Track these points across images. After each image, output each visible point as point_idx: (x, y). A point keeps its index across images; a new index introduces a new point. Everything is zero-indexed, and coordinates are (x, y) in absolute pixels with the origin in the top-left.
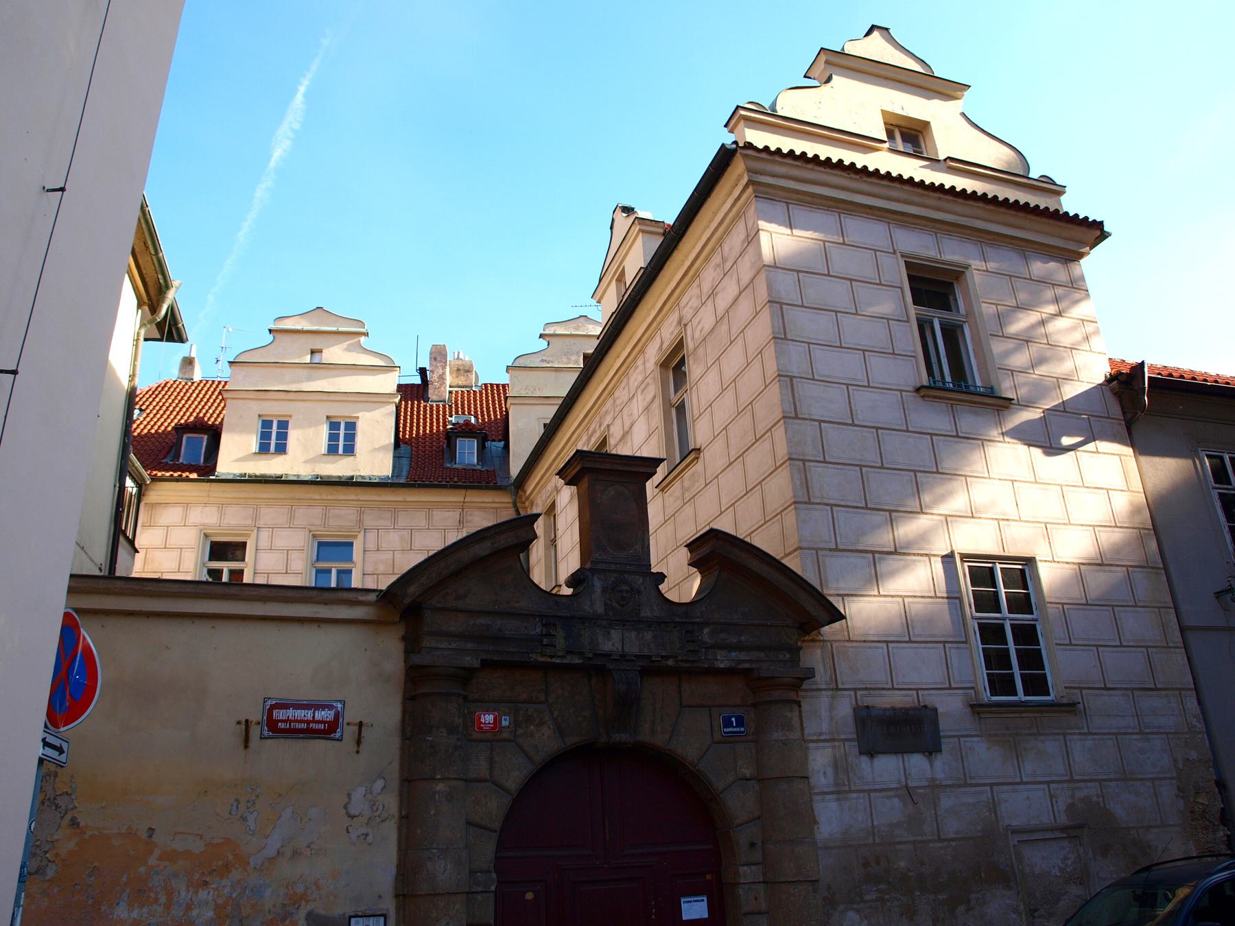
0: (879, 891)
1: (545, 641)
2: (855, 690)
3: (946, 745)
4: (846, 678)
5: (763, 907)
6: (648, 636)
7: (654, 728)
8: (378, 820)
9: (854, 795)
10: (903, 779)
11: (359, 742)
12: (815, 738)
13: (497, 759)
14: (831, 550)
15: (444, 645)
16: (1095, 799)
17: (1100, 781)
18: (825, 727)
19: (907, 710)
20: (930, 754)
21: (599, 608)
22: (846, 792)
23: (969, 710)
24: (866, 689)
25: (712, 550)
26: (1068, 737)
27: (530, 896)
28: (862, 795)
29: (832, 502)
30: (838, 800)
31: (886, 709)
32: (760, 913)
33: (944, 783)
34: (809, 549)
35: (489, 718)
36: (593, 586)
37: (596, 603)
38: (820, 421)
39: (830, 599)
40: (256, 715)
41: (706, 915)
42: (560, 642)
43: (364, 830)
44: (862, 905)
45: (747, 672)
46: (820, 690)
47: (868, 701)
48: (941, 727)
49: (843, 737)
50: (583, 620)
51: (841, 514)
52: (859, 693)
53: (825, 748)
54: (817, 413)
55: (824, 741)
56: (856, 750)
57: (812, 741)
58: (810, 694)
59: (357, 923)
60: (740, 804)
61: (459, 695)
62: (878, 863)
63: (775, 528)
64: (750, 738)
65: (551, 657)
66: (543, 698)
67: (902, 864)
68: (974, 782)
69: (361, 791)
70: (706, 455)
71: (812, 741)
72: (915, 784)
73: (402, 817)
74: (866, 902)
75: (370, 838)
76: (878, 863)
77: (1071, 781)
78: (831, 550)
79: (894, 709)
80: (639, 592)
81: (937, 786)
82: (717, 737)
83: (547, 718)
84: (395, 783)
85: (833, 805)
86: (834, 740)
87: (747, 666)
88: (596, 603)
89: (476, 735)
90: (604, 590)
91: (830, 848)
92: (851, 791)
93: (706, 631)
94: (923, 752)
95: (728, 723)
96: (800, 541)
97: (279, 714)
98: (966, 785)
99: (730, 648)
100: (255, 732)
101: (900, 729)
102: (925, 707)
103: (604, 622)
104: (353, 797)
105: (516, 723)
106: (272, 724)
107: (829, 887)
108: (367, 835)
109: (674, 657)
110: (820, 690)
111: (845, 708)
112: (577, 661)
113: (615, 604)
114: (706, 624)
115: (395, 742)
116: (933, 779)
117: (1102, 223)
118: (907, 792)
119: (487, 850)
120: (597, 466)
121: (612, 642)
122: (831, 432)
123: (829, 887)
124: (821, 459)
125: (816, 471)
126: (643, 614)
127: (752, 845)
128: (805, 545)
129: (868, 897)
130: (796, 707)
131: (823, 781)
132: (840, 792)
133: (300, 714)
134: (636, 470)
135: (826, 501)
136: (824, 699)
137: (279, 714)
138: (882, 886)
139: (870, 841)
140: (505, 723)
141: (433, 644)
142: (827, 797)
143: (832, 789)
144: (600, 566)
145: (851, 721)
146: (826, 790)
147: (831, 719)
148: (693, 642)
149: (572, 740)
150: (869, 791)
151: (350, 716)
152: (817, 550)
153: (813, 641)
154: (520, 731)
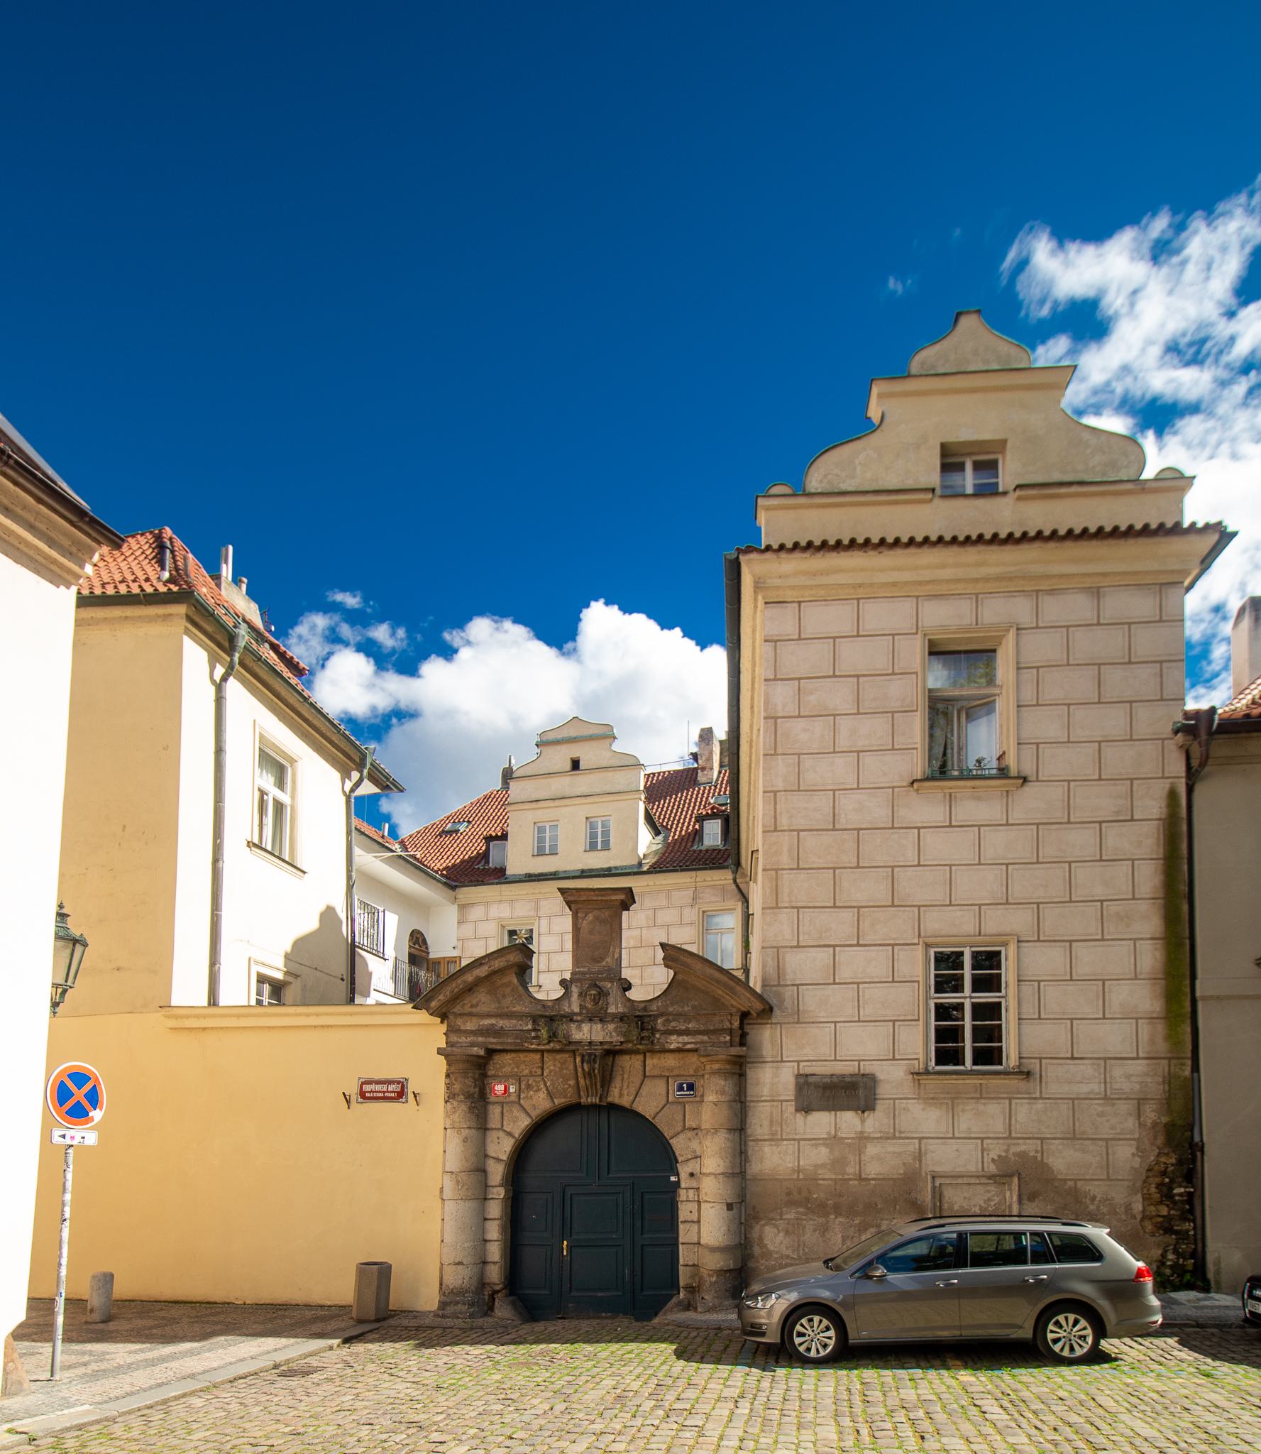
2: (798, 1062)
3: (880, 1106)
6: (611, 1027)
7: (620, 1094)
16: (1032, 1154)
17: (1042, 1139)
19: (843, 1076)
25: (673, 955)
26: (1014, 1102)
29: (800, 904)
40: (353, 1090)
47: (808, 1071)
50: (563, 1016)
67: (822, 1195)
77: (1010, 1137)
81: (867, 1138)
90: (580, 995)
94: (855, 1109)
95: (680, 1088)
97: (367, 1088)
98: (894, 1138)
100: (354, 1098)
101: (847, 1091)
106: (363, 1095)
114: (661, 1015)
117: (1220, 523)
118: (834, 1140)
121: (585, 1032)
122: (809, 840)
128: (768, 945)
129: (788, 1216)
133: (379, 1087)
137: (367, 1088)
138: (801, 1210)
139: (795, 1176)
140: (512, 1090)
149: (559, 1102)
150: (799, 1140)
151: (411, 1088)
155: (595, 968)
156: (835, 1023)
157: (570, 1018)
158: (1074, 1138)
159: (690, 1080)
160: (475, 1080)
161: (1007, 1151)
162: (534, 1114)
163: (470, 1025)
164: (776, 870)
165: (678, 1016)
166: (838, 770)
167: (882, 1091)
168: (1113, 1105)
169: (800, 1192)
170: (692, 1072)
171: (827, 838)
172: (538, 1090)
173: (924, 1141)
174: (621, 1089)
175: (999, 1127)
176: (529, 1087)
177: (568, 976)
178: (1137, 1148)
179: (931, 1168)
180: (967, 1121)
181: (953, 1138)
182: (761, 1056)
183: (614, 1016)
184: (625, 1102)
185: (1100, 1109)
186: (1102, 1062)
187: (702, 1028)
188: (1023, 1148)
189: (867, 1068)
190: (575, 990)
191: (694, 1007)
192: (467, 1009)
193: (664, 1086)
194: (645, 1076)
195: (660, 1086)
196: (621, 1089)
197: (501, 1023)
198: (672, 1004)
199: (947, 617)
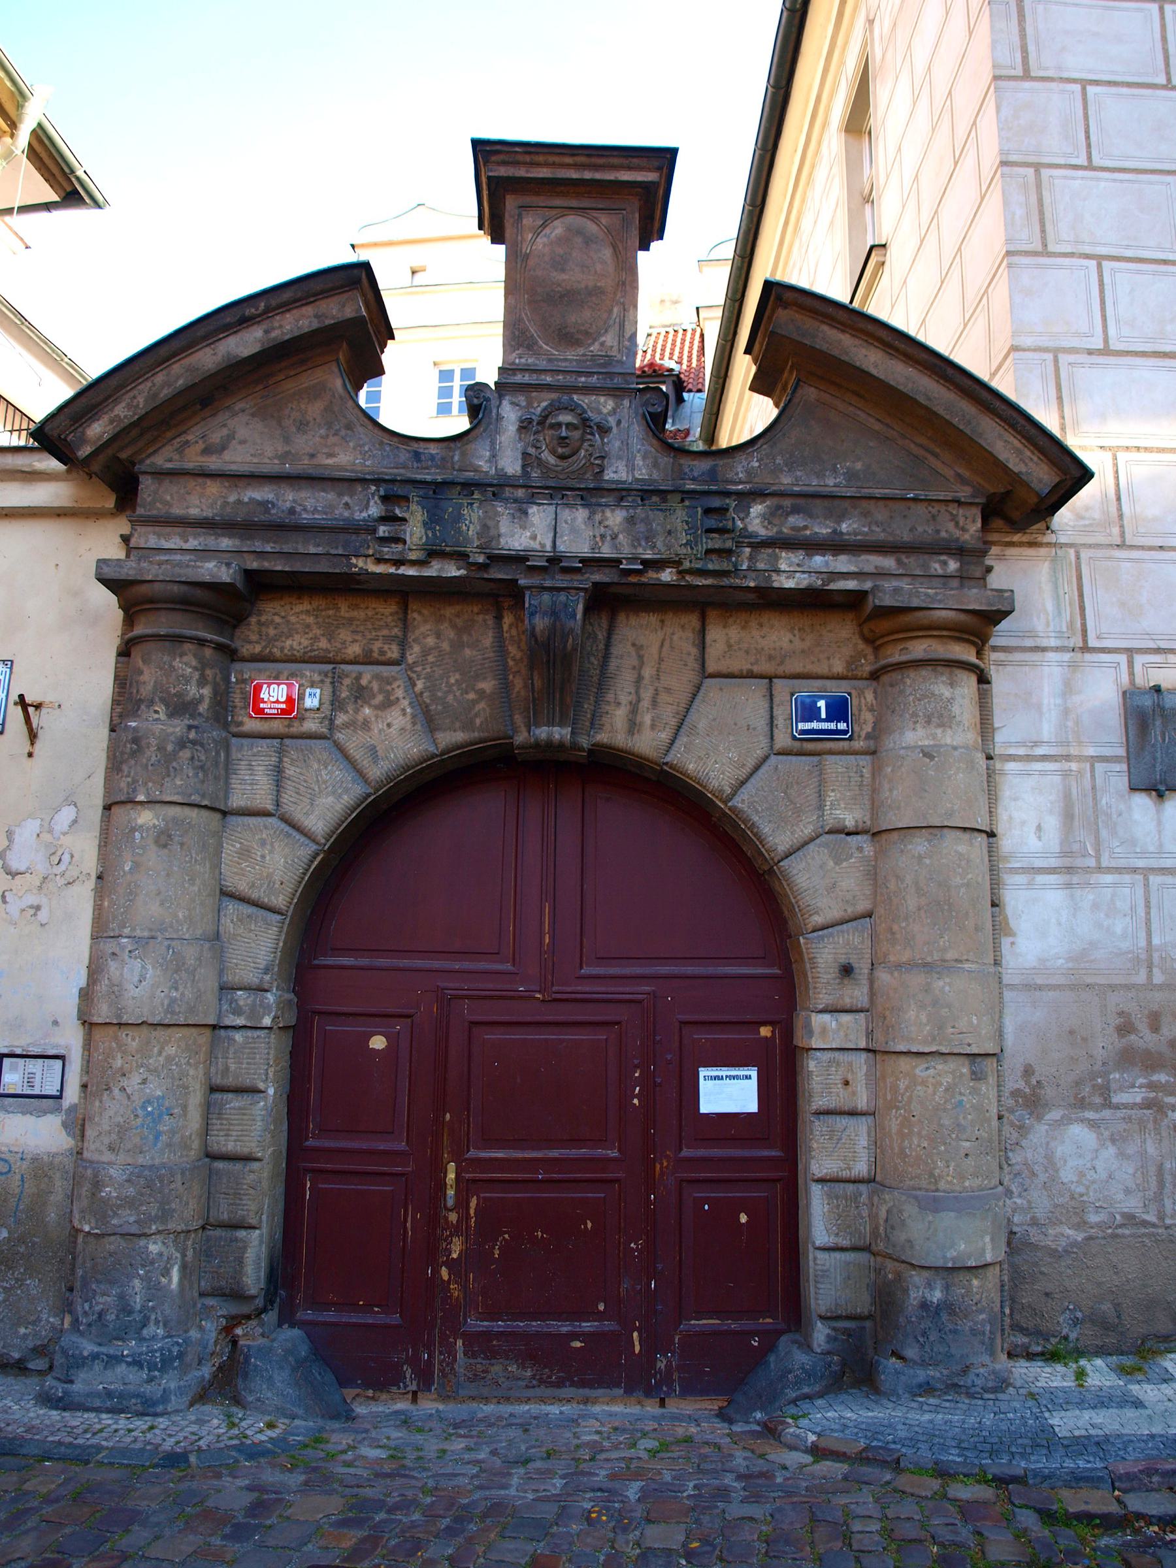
0: (1151, 1086)
1: (383, 530)
4: (1107, 621)
5: (862, 1101)
6: (616, 518)
8: (61, 881)
9: (1108, 878)
11: (33, 736)
12: (1021, 751)
13: (290, 771)
14: (1090, 352)
15: (175, 542)
18: (1047, 729)
21: (511, 465)
22: (1087, 870)
24: (1158, 651)
27: (378, 1043)
28: (1127, 878)
30: (1069, 886)
32: (853, 1113)
35: (274, 694)
36: (499, 418)
37: (506, 455)
41: (753, 1107)
42: (415, 531)
43: (32, 899)
44: (1107, 1113)
45: (853, 602)
46: (1044, 649)
49: (1091, 751)
50: (469, 487)
51: (1120, 278)
52: (1139, 660)
54: (1078, 64)
55: (1044, 758)
56: (1123, 782)
58: (1018, 656)
59: (14, 1069)
60: (822, 885)
61: (201, 642)
62: (1155, 1028)
63: (978, 329)
64: (858, 744)
65: (398, 563)
66: (393, 652)
69: (32, 826)
70: (893, 253)
73: (99, 877)
74: (1117, 1107)
75: (43, 916)
76: (1155, 1028)
78: (1090, 352)
80: (604, 430)
82: (782, 740)
83: (400, 693)
84: (96, 814)
86: (1067, 758)
87: (851, 585)
88: (506, 455)
89: (251, 725)
90: (524, 426)
91: (1040, 988)
92: (1100, 869)
93: (757, 509)
96: (1015, 334)
99: (813, 546)
103: (520, 493)
104: (17, 837)
105: (336, 703)
107: (1028, 1071)
108: (38, 908)
109: (676, 563)
110: (1044, 649)
111: (1102, 690)
112: (453, 571)
113: (547, 457)
114: (758, 494)
115: (102, 734)
119: (258, 947)
120: (521, 172)
123: (1028, 1071)
124: (1082, 160)
125: (1066, 190)
126: (609, 475)
127: (847, 971)
128: (1028, 341)
130: (969, 683)
132: (1070, 869)
134: (610, 176)
135: (1087, 250)
136: (1049, 674)
138: (1162, 1077)
139: (1141, 978)
140: (311, 702)
141: (153, 542)
142: (1041, 879)
143: (1053, 863)
144: (518, 378)
145: (1114, 720)
146: (1038, 863)
147: (1066, 712)
148: (722, 531)
149: (451, 737)
150: (1147, 872)
152: (1056, 352)
153: (1032, 544)
154: (341, 718)
155: (571, 356)
157: (495, 488)
159: (839, 689)
160: (203, 666)
162: (377, 772)
163: (200, 501)
164: (1037, 167)
165: (805, 500)
170: (839, 667)
172: (388, 703)
174: (634, 709)
176: (361, 694)
177: (489, 376)
183: (621, 494)
184: (647, 742)
187: (880, 535)
190: (510, 414)
191: (851, 475)
192: (193, 459)
193: (764, 704)
194: (704, 674)
195: (748, 703)
196: (634, 709)
197: (288, 497)
198: (791, 465)
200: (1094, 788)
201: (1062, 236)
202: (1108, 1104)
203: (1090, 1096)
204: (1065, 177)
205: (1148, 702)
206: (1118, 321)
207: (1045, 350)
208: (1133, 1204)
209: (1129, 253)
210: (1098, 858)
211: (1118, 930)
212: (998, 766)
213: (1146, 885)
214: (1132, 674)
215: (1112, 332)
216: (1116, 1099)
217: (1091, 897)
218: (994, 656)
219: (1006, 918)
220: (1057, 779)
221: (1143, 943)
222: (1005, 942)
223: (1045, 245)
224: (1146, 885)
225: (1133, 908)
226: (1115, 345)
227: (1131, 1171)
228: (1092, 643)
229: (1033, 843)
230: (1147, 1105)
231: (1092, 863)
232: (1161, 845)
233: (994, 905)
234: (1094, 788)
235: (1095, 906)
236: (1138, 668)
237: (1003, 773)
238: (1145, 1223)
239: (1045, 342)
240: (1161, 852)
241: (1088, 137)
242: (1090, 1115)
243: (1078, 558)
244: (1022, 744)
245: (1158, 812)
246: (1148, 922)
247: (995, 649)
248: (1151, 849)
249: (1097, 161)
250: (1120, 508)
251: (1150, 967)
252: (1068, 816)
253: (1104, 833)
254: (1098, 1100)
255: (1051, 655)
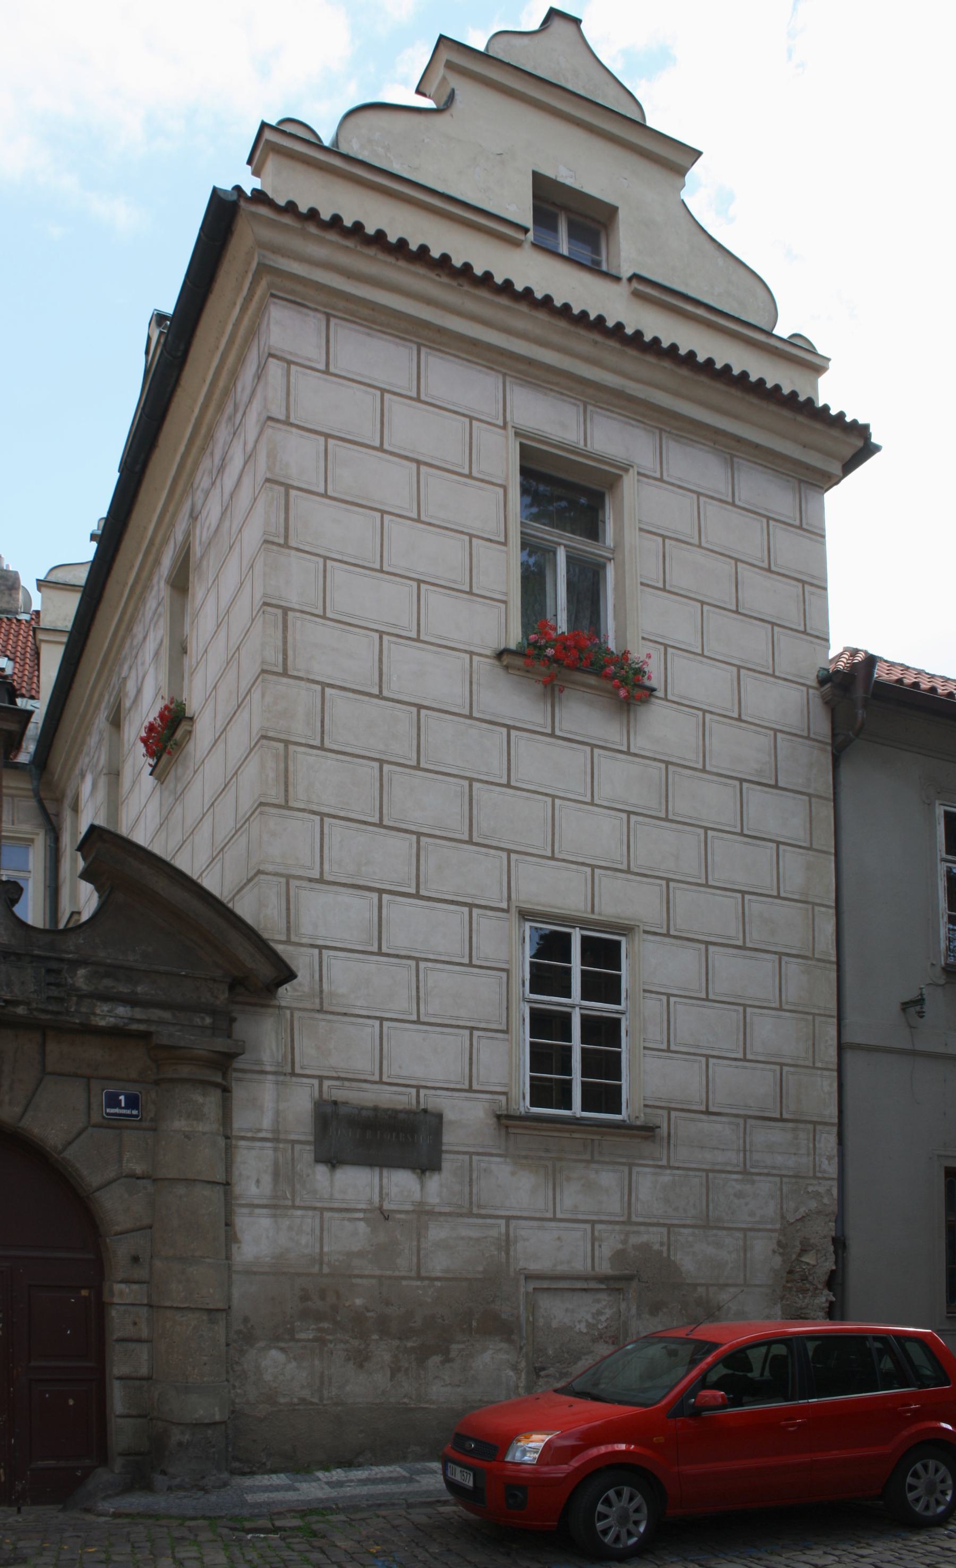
0: (320, 1330)
2: (321, 1078)
3: (448, 1163)
9: (299, 1213)
10: (376, 1199)
12: (249, 1135)
14: (311, 880)
18: (267, 1122)
19: (396, 1112)
20: (423, 1172)
22: (286, 1207)
23: (495, 1120)
24: (338, 1078)
28: (310, 1213)
30: (274, 1216)
31: (363, 1108)
33: (437, 1209)
34: (276, 874)
38: (324, 685)
39: (272, 944)
44: (291, 1344)
48: (446, 1139)
51: (336, 830)
52: (327, 1083)
53: (262, 1148)
57: (243, 1138)
58: (248, 1076)
68: (483, 1212)
71: (243, 1138)
72: (393, 1207)
79: (376, 1109)
81: (431, 1213)
85: (266, 1222)
91: (255, 1273)
92: (294, 1207)
94: (413, 1168)
102: (425, 1111)
111: (300, 1102)
116: (421, 1203)
123: (246, 1320)
124: (317, 743)
129: (302, 1336)
131: (254, 1190)
132: (276, 1207)
138: (325, 1325)
139: (316, 1269)
142: (257, 1211)
143: (265, 1202)
146: (256, 1202)
150: (322, 1210)
152: (288, 877)
156: (382, 1019)
158: (706, 1227)
161: (624, 1242)
166: (388, 603)
167: (449, 1138)
168: (753, 1182)
169: (323, 1295)
171: (374, 708)
173: (513, 1223)
175: (614, 1205)
178: (779, 1243)
179: (522, 1264)
180: (571, 1198)
181: (554, 1219)
182: (259, 1062)
185: (739, 1187)
186: (741, 1121)
188: (645, 1238)
189: (432, 1101)
199: (554, 420)
200: (293, 1159)
201: (299, 796)
202: (293, 1339)
203: (282, 1335)
204: (305, 753)
205: (329, 1110)
206: (330, 861)
207: (281, 875)
208: (306, 1393)
209: (342, 814)
210: (293, 1201)
211: (303, 1242)
212: (234, 1142)
213: (322, 1218)
214: (321, 1091)
215: (326, 867)
216: (298, 1336)
217: (288, 1223)
218: (235, 1075)
219: (235, 1233)
220: (271, 1152)
221: (317, 1250)
222: (234, 1247)
223: (287, 801)
224: (322, 1218)
225: (313, 1230)
226: (327, 877)
227: (304, 1375)
228: (298, 1071)
229: (254, 1190)
230: (315, 1340)
231: (289, 1203)
232: (332, 1195)
233: (227, 1225)
234: (293, 1159)
235: (290, 1228)
236: (325, 1088)
237: (236, 1147)
238: (312, 1403)
239: (281, 870)
240: (331, 1198)
241: (322, 726)
242: (282, 1345)
243: (292, 1016)
244: (250, 1130)
245: (331, 1175)
246: (321, 1239)
247: (236, 1070)
248: (326, 1197)
249: (327, 744)
250: (321, 986)
251: (321, 1264)
252: (276, 1175)
253: (298, 1186)
254: (287, 1337)
255: (270, 1077)
